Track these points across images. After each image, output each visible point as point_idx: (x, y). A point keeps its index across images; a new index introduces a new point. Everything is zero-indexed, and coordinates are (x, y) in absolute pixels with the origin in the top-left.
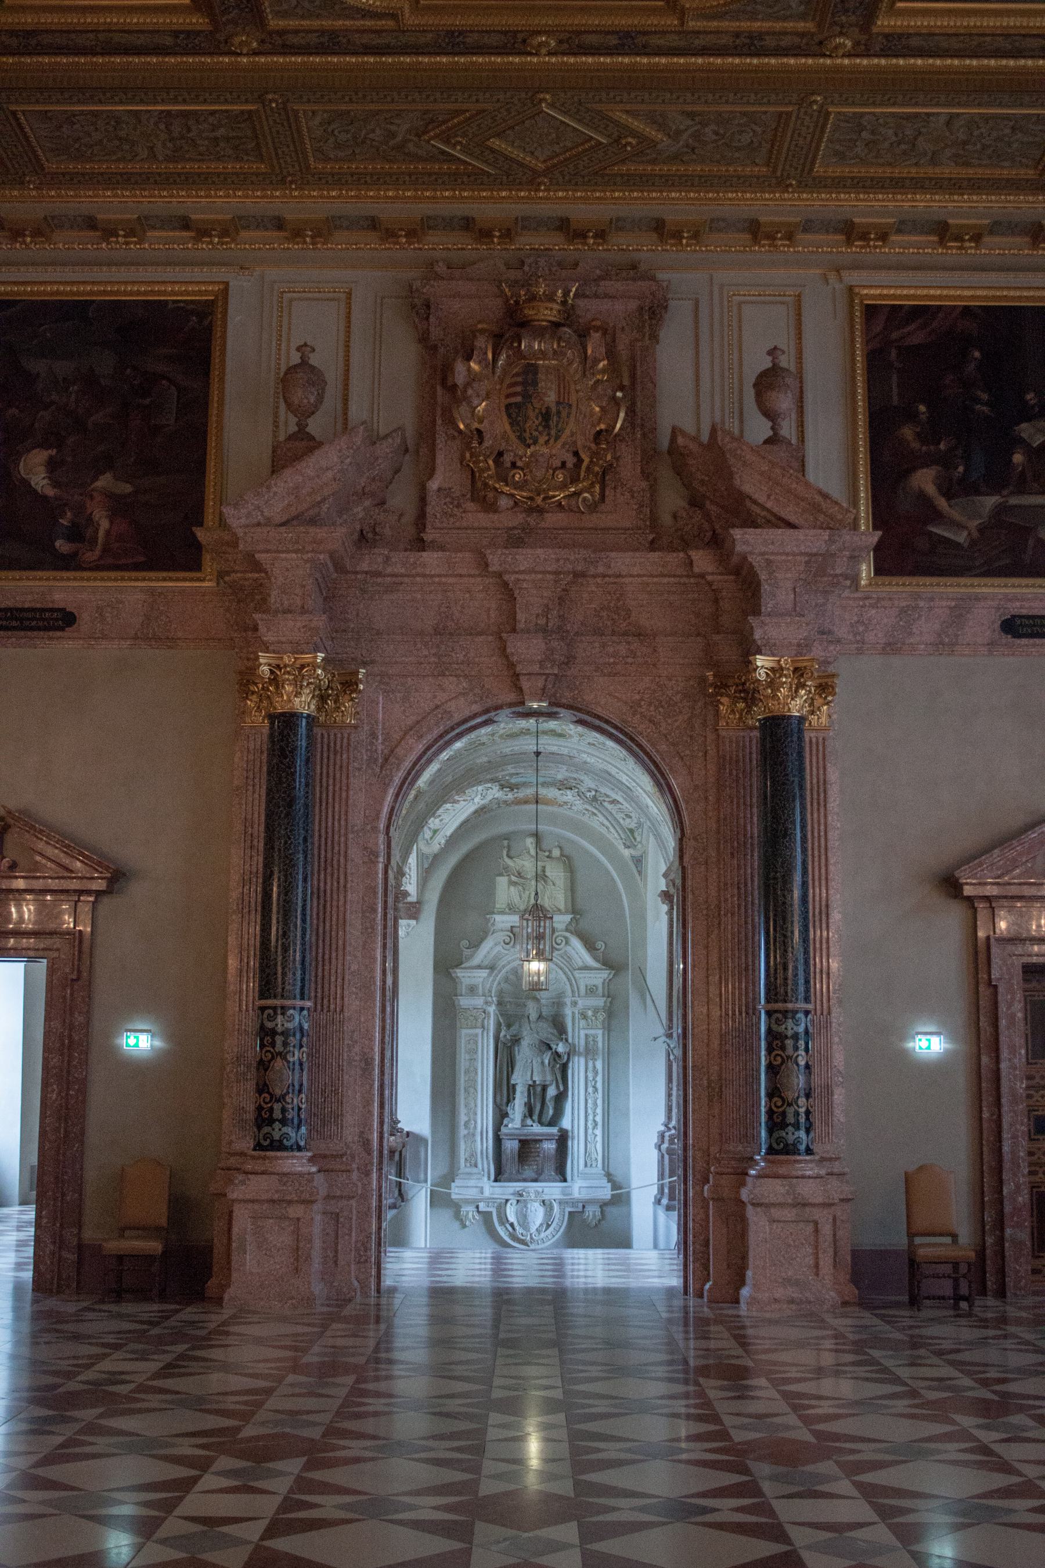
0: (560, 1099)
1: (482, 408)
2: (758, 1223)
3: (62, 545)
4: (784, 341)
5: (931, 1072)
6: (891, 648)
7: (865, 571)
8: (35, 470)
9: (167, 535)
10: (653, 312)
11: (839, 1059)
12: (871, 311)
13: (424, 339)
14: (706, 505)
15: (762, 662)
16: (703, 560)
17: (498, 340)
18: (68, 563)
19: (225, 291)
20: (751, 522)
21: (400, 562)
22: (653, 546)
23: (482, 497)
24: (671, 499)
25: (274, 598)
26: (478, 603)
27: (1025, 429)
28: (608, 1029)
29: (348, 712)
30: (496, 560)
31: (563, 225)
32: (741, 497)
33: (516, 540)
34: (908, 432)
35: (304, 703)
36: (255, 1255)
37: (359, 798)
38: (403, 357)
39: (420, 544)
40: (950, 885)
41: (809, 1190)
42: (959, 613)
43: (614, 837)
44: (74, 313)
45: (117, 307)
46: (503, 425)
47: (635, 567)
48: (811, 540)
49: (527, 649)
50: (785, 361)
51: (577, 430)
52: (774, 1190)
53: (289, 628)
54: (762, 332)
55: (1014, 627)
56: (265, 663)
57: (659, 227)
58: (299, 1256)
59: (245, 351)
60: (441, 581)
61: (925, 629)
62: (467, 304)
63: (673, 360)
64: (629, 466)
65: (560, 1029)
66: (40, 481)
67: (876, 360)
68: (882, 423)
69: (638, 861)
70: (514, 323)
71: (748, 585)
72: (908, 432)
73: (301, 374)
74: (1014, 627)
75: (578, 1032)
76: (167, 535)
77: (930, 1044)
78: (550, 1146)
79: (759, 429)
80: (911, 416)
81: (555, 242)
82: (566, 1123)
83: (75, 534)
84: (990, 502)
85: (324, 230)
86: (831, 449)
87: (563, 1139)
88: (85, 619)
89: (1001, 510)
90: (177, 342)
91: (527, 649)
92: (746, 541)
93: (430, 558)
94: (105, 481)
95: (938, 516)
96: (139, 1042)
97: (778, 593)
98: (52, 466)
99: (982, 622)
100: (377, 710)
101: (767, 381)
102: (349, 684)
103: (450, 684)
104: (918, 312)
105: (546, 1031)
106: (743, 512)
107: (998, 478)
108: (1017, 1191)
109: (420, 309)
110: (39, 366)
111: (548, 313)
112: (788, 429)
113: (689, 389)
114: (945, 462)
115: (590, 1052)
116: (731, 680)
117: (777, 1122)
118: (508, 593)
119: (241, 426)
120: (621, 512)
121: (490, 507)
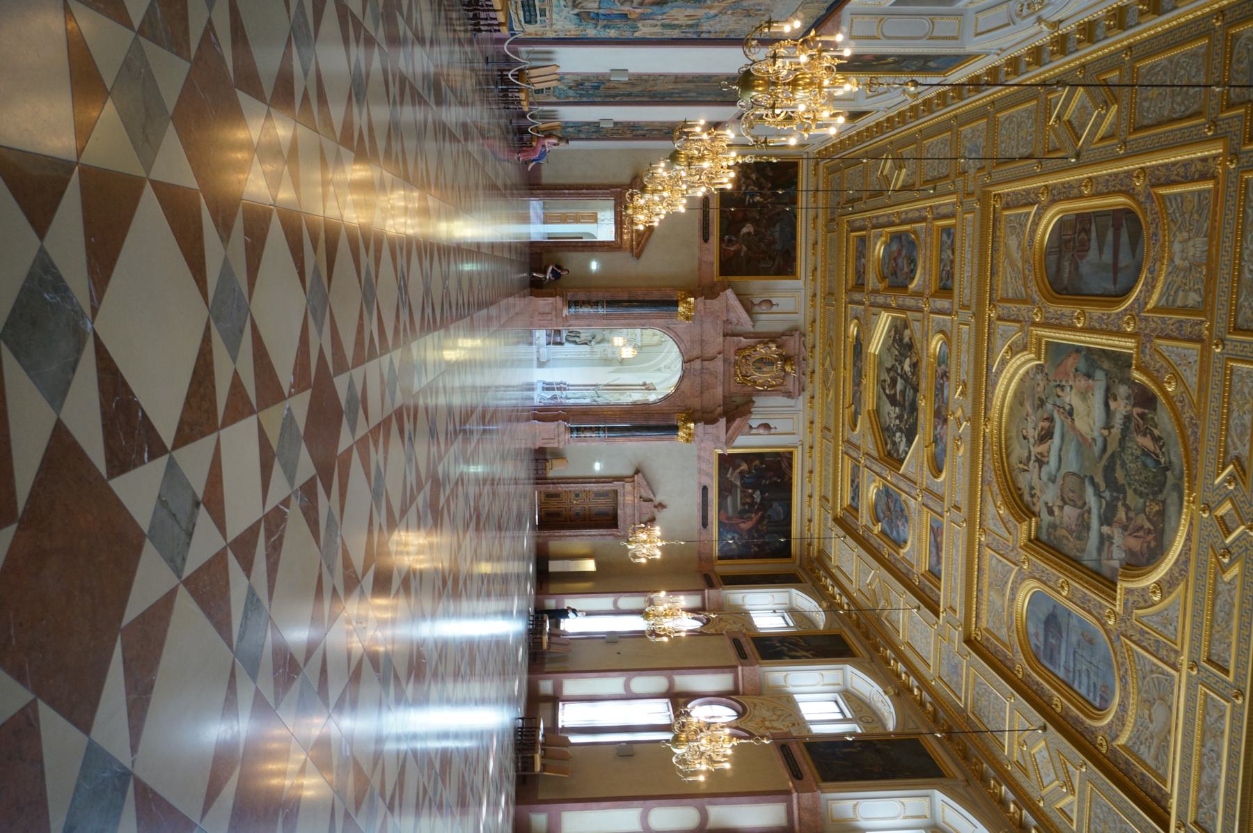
0: (575, 342)
1: (761, 350)
2: (552, 425)
4: (778, 431)
5: (591, 466)
6: (699, 457)
7: (720, 451)
8: (748, 229)
9: (730, 266)
10: (789, 395)
11: (594, 444)
12: (791, 453)
13: (783, 334)
14: (735, 411)
15: (692, 425)
16: (720, 410)
17: (780, 355)
18: (722, 240)
20: (730, 421)
21: (720, 331)
22: (724, 397)
23: (739, 350)
24: (738, 400)
25: (709, 301)
26: (711, 350)
27: (758, 493)
28: (600, 359)
30: (720, 356)
32: (734, 419)
33: (725, 361)
34: (757, 462)
36: (544, 303)
37: (658, 321)
38: (779, 327)
39: (725, 335)
40: (637, 472)
41: (562, 437)
42: (709, 475)
43: (668, 361)
44: (794, 237)
45: (794, 248)
46: (758, 357)
47: (719, 392)
48: (723, 437)
49: (697, 364)
50: (773, 431)
52: (562, 429)
53: (700, 306)
54: (779, 425)
55: (705, 489)
57: (813, 397)
60: (716, 341)
61: (704, 466)
62: (792, 345)
63: (781, 400)
65: (599, 343)
66: (745, 230)
67: (778, 454)
68: (760, 456)
69: (659, 370)
71: (713, 421)
72: (757, 462)
74: (705, 489)
75: (598, 348)
76: (730, 266)
77: (597, 467)
78: (558, 340)
79: (755, 424)
80: (762, 463)
81: (810, 370)
82: (567, 345)
83: (730, 241)
84: (738, 483)
86: (749, 442)
87: (561, 344)
88: (706, 245)
89: (736, 486)
90: (785, 265)
91: (697, 364)
92: (723, 421)
93: (721, 339)
94: (744, 248)
95: (734, 469)
96: (594, 266)
97: (710, 428)
98: (749, 233)
99: (705, 481)
101: (766, 426)
102: (688, 318)
103: (688, 345)
104: (790, 466)
105: (599, 338)
106: (730, 421)
107: (745, 486)
108: (562, 488)
109: (790, 332)
110: (778, 227)
111: (788, 369)
112: (754, 431)
113: (766, 405)
114: (749, 472)
115: (592, 353)
117: (578, 429)
118: (712, 359)
119: (756, 285)
120: (733, 389)
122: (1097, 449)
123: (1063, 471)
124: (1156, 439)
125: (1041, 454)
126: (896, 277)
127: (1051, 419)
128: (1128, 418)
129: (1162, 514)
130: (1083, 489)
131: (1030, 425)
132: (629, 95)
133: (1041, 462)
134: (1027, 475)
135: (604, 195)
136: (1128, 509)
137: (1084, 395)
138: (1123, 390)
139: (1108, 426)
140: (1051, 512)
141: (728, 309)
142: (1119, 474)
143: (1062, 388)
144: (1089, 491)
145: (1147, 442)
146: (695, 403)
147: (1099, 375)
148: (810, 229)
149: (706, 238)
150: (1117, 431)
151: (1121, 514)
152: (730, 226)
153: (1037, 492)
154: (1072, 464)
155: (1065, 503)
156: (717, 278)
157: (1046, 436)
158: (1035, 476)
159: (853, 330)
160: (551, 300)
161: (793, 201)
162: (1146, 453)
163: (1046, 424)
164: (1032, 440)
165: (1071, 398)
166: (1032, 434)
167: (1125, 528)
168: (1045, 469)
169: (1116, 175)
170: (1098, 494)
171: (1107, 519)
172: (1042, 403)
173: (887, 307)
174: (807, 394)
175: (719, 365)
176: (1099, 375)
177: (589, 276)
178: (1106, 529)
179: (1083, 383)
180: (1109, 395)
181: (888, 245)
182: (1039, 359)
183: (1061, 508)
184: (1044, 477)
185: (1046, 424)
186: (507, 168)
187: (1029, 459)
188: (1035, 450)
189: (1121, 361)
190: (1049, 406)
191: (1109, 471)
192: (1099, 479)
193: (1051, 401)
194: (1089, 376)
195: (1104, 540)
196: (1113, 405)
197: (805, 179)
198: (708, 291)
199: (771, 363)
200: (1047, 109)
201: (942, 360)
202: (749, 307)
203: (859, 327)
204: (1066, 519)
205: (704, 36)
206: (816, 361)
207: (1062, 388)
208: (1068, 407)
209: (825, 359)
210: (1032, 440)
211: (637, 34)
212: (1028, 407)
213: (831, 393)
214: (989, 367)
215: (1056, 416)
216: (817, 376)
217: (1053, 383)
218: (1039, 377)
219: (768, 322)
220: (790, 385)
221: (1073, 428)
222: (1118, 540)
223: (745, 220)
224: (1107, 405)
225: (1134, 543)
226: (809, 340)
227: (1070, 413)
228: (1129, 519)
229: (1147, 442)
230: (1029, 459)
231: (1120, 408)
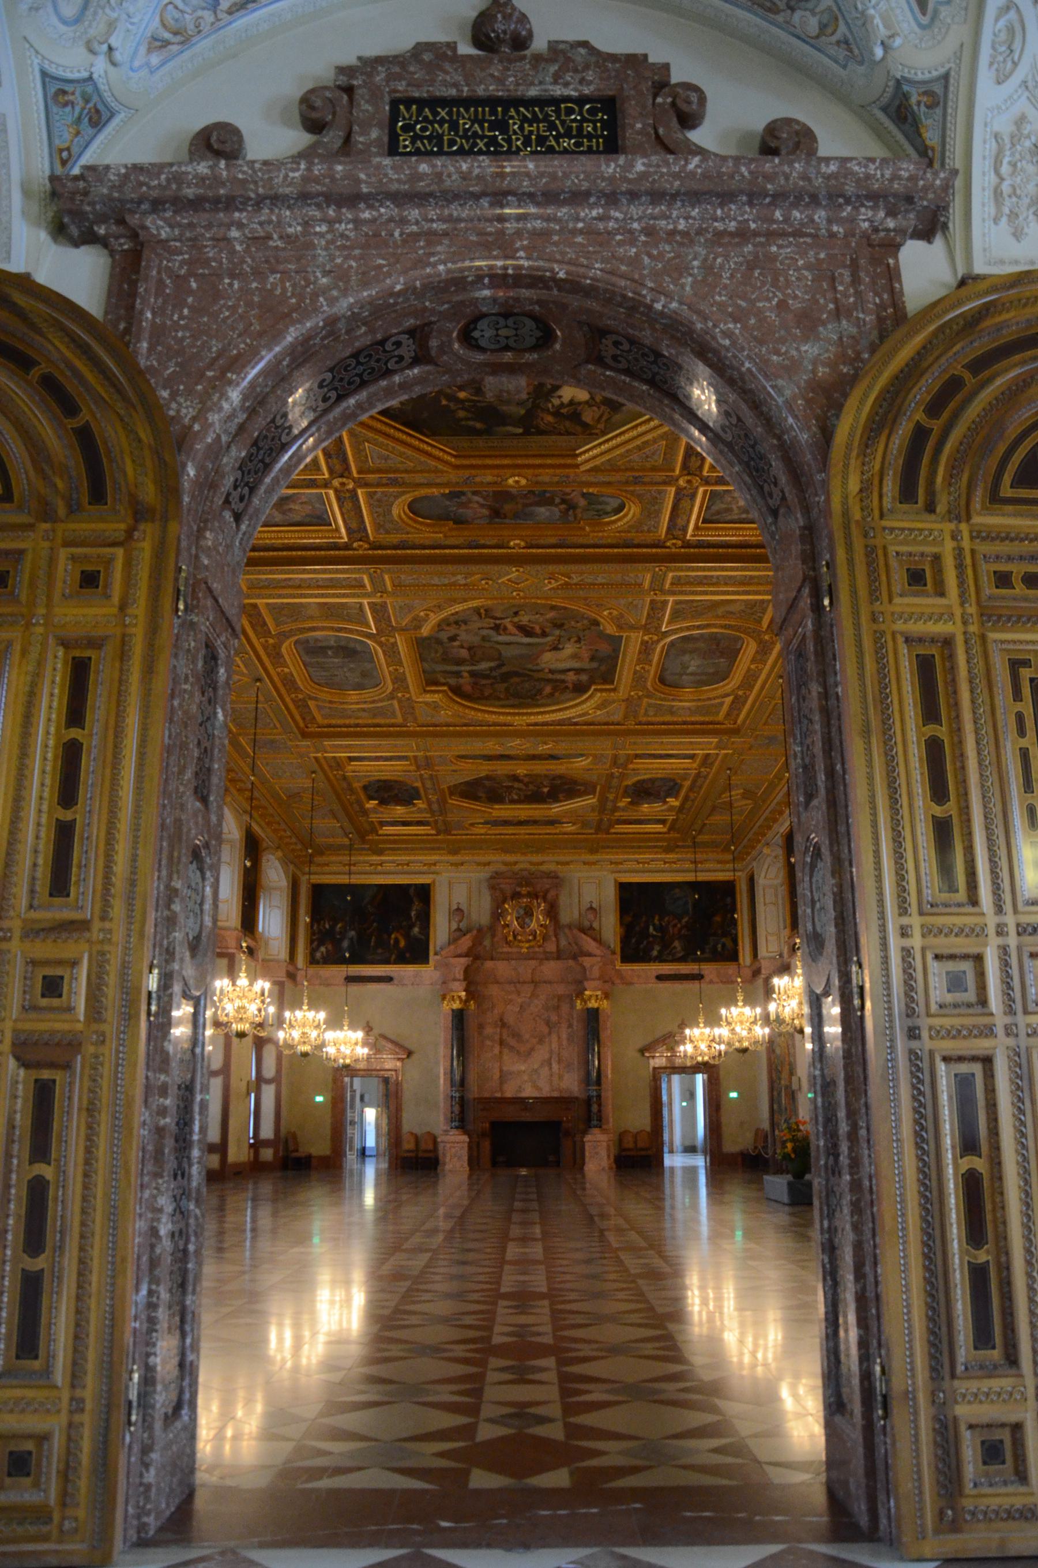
122: (530, 666)
124: (552, 695)
125: (505, 629)
127: (544, 634)
128: (563, 681)
129: (499, 699)
130: (490, 659)
131: (533, 618)
133: (496, 628)
134: (475, 618)
137: (575, 656)
138: (584, 677)
139: (551, 671)
140: (453, 639)
142: (516, 680)
143: (579, 641)
144: (492, 664)
145: (548, 690)
147: (595, 665)
150: (550, 676)
151: (484, 682)
153: (463, 627)
154: (508, 652)
155: (470, 649)
157: (526, 631)
158: (479, 625)
162: (540, 691)
163: (538, 630)
164: (516, 619)
165: (569, 649)
166: (524, 619)
167: (475, 684)
168: (492, 633)
169: (756, 681)
170: (491, 669)
171: (473, 674)
172: (560, 626)
176: (595, 665)
178: (466, 674)
179: (586, 655)
180: (578, 671)
183: (462, 647)
184: (485, 632)
185: (538, 630)
187: (496, 618)
188: (507, 622)
190: (557, 632)
191: (516, 674)
192: (504, 669)
193: (563, 633)
194: (592, 659)
195: (458, 674)
196: (571, 673)
204: (455, 650)
207: (579, 641)
210: (516, 619)
212: (551, 615)
215: (549, 639)
217: (581, 634)
218: (585, 622)
221: (543, 651)
222: (462, 681)
224: (569, 670)
225: (468, 688)
227: (556, 648)
230: (496, 618)
231: (571, 677)
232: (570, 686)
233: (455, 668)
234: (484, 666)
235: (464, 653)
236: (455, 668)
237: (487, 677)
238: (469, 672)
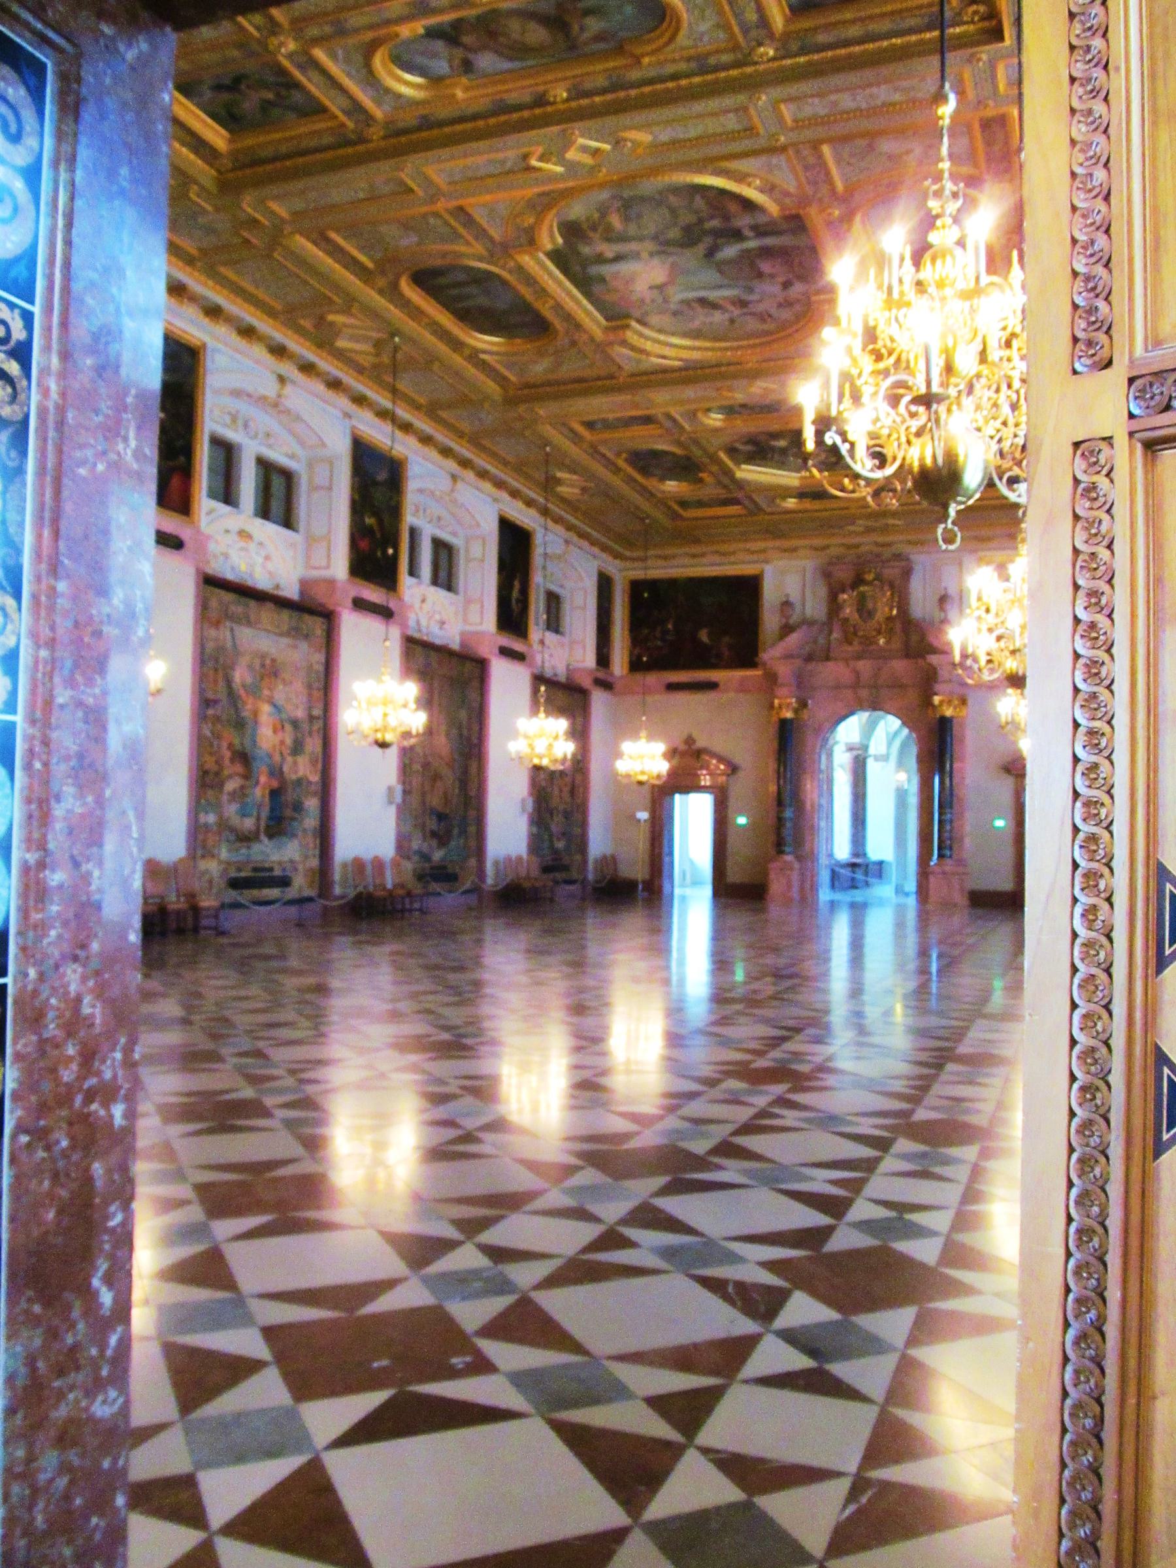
3: (713, 660)
8: (704, 636)
10: (907, 573)
15: (936, 699)
18: (714, 666)
19: (762, 572)
25: (780, 681)
29: (805, 714)
31: (876, 544)
33: (859, 657)
35: (789, 715)
38: (823, 592)
39: (828, 659)
51: (880, 616)
56: (776, 702)
58: (789, 886)
59: (770, 593)
60: (831, 672)
62: (844, 574)
64: (898, 626)
70: (858, 581)
73: (786, 604)
85: (794, 550)
90: (747, 589)
91: (864, 693)
96: (742, 820)
98: (709, 635)
100: (817, 710)
109: (827, 575)
116: (927, 703)
118: (857, 674)
119: (770, 621)
120: (897, 644)
121: (850, 644)
123: (726, 282)
126: (685, 467)
128: (608, 240)
132: (464, 782)
133: (743, 304)
135: (661, 805)
136: (701, 221)
138: (586, 250)
140: (786, 285)
141: (788, 656)
146: (912, 696)
148: (704, 560)
149: (712, 686)
151: (715, 223)
152: (704, 658)
156: (758, 673)
159: (791, 503)
160: (772, 876)
161: (673, 583)
168: (746, 297)
171: (737, 235)
173: (729, 474)
174: (906, 549)
175: (865, 666)
177: (752, 826)
178: (747, 232)
181: (663, 479)
182: (628, 326)
183: (772, 276)
186: (633, 921)
189: (557, 257)
197: (658, 571)
198: (772, 679)
199: (862, 599)
200: (375, 366)
201: (730, 411)
202: (787, 629)
203: (784, 498)
205: (317, 712)
206: (867, 543)
208: (655, 291)
209: (851, 533)
211: (315, 778)
213: (891, 521)
214: (680, 369)
216: (880, 539)
219: (814, 606)
220: (890, 572)
223: (695, 639)
226: (834, 551)
228: (712, 217)
229: (616, 221)
232: (591, 234)
233: (769, 241)
234: (730, 251)
235: (766, 267)
236: (769, 241)
237: (717, 233)
238: (746, 239)
